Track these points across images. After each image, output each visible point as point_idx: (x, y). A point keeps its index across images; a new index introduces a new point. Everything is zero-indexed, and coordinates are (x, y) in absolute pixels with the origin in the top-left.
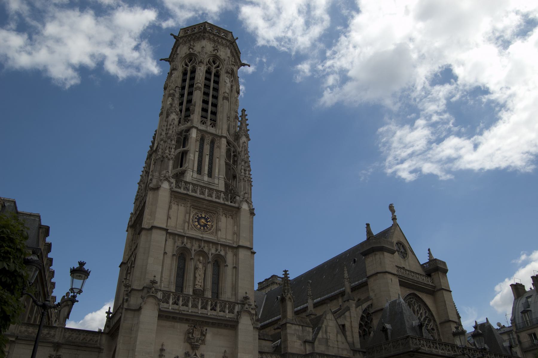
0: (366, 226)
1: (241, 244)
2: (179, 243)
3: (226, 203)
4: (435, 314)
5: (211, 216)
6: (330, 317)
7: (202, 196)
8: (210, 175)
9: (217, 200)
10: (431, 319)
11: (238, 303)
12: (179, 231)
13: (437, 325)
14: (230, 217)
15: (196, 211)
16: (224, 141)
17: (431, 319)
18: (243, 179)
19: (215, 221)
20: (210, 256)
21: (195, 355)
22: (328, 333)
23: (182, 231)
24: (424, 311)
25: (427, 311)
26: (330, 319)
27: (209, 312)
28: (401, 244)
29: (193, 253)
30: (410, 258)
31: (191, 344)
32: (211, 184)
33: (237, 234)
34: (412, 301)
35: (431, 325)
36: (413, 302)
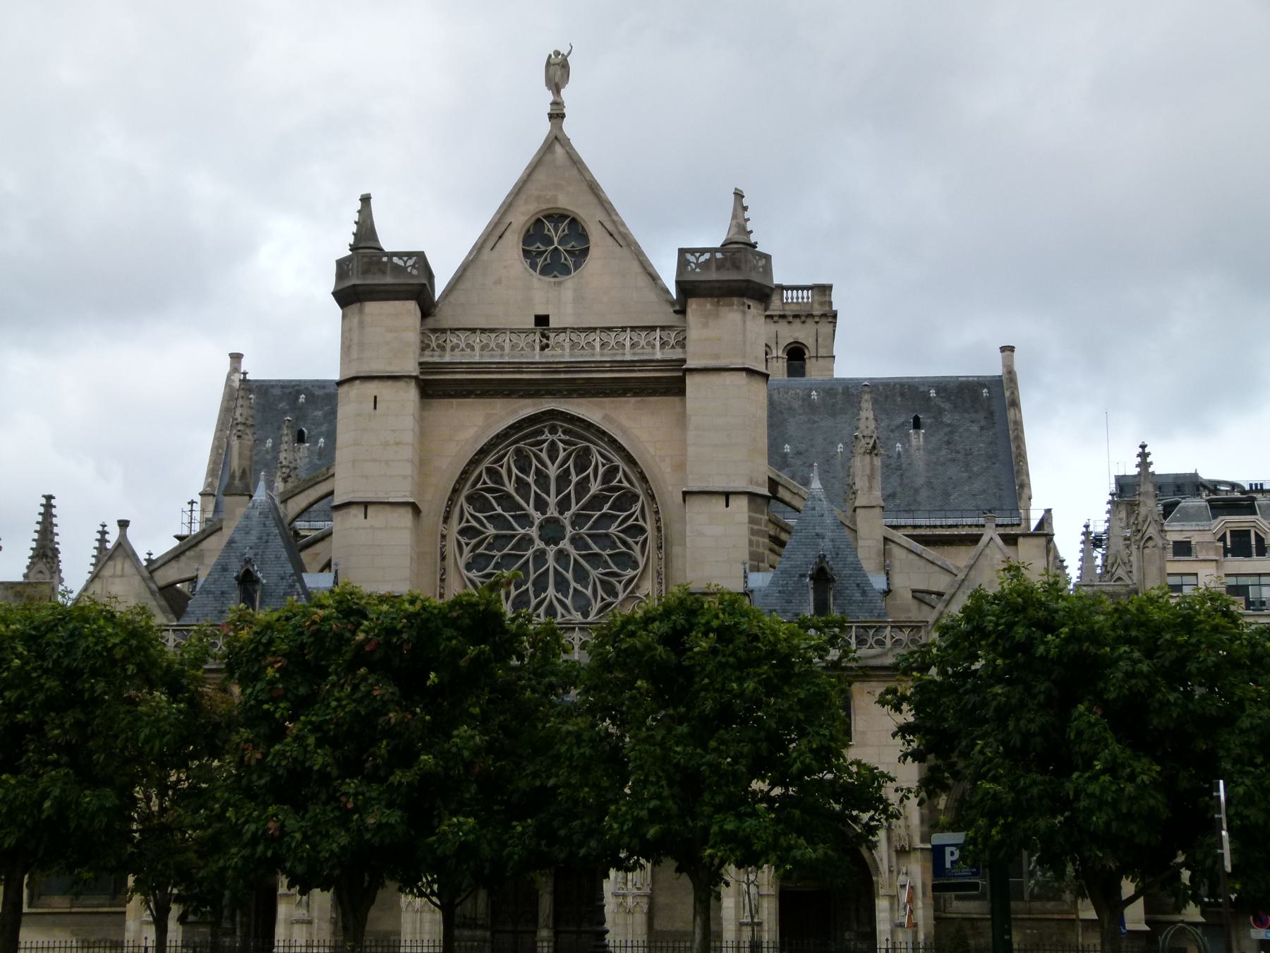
0: (358, 205)
4: (669, 470)
6: (119, 566)
10: (639, 491)
13: (657, 512)
24: (601, 470)
25: (617, 461)
26: (119, 572)
28: (567, 217)
30: (593, 263)
34: (544, 441)
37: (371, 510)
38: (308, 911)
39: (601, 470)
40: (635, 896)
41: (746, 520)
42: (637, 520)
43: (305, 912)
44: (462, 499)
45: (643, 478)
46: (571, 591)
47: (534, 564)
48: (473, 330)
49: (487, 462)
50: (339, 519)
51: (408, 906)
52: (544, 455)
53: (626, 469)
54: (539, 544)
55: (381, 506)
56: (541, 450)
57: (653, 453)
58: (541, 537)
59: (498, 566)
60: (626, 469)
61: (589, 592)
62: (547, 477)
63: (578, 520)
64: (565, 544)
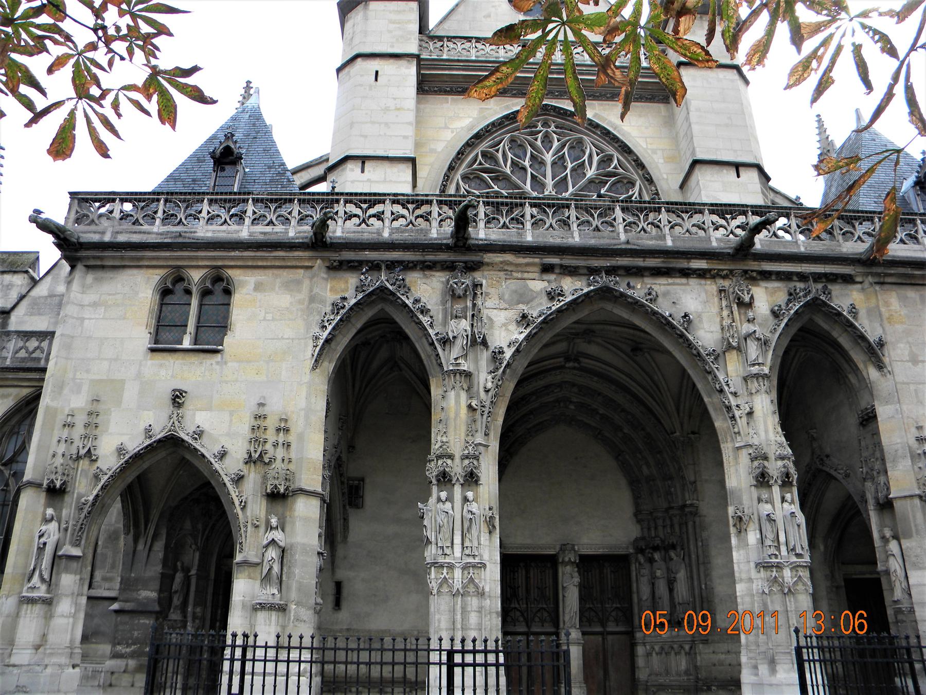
4: (661, 161)
10: (636, 177)
17: (636, 177)
37: (368, 165)
38: (280, 591)
39: (596, 159)
40: (795, 567)
43: (276, 592)
44: (458, 176)
45: (640, 165)
48: (468, 39)
49: (484, 146)
51: (441, 585)
53: (620, 157)
55: (379, 162)
57: (645, 147)
60: (620, 157)
62: (542, 163)
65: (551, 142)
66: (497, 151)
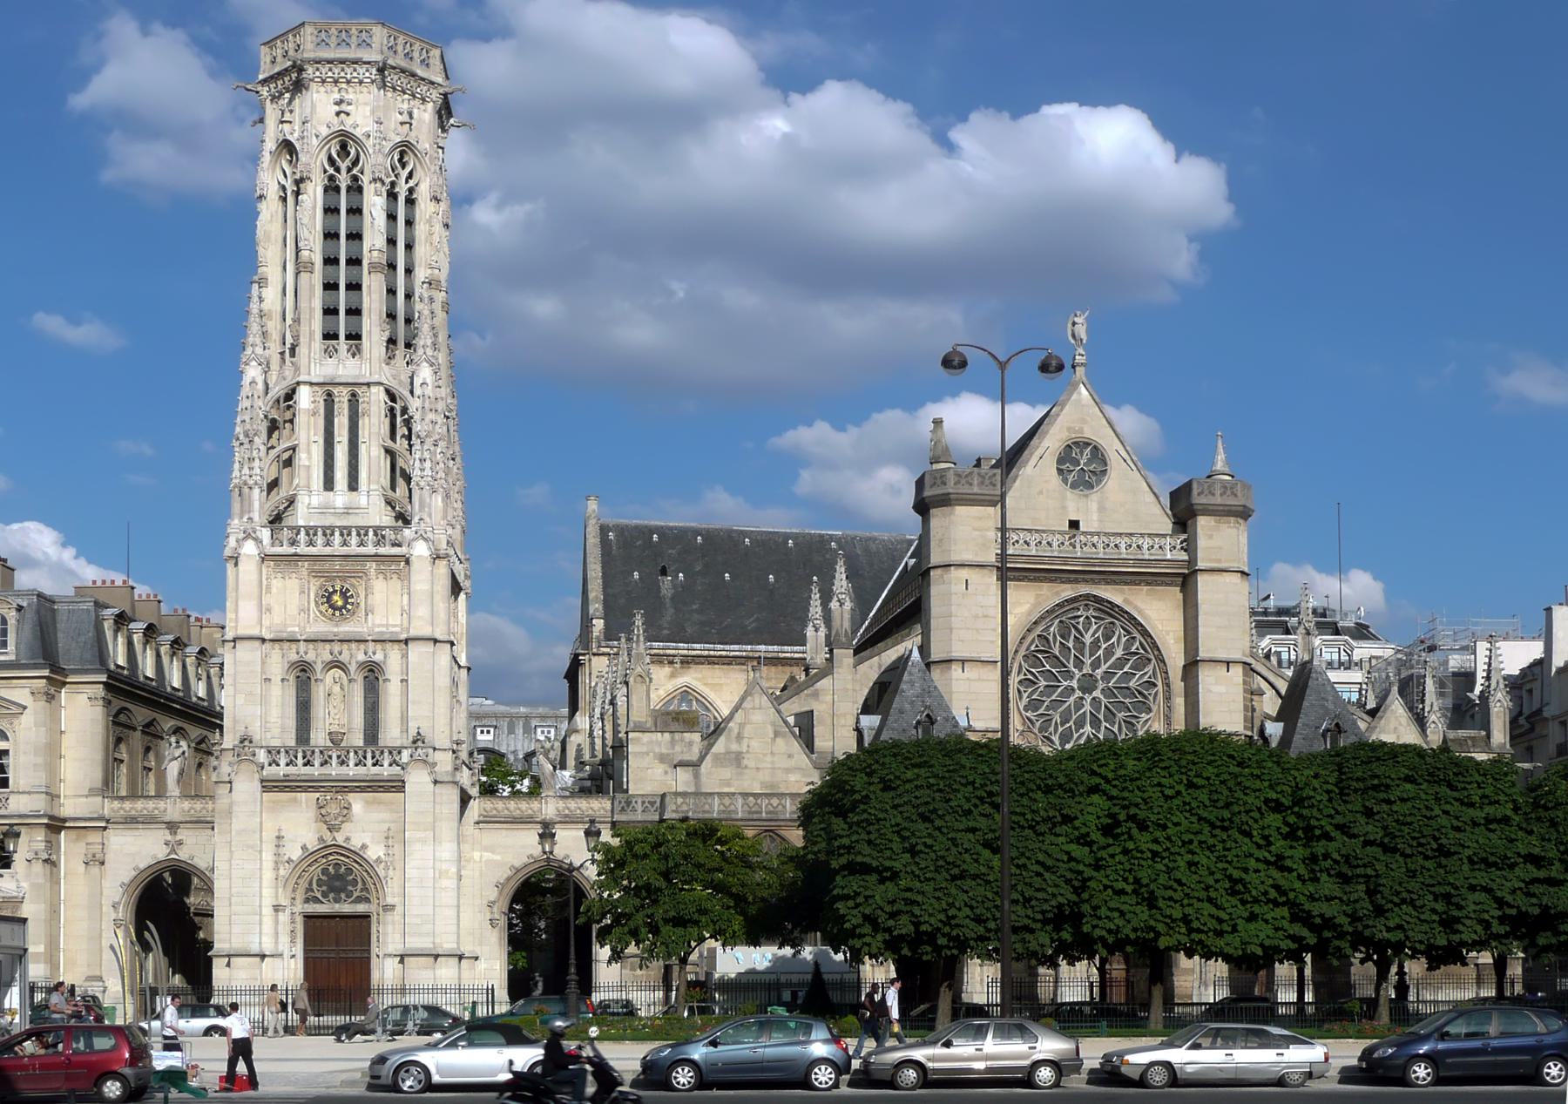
1: (413, 633)
2: (294, 657)
3: (382, 550)
4: (1172, 641)
5: (353, 586)
7: (328, 550)
8: (353, 485)
9: (362, 550)
11: (406, 748)
12: (293, 629)
13: (1166, 673)
14: (395, 576)
15: (322, 579)
16: (378, 395)
17: (1153, 657)
18: (418, 485)
19: (362, 596)
20: (353, 668)
21: (334, 839)
22: (746, 740)
23: (297, 629)
24: (1124, 639)
27: (351, 770)
29: (319, 667)
31: (325, 822)
32: (350, 511)
33: (407, 613)
34: (1079, 617)
35: (1146, 673)
36: (1081, 619)
41: (1241, 682)
42: (1150, 677)
45: (1155, 646)
46: (1103, 728)
47: (1070, 711)
50: (938, 671)
52: (1080, 627)
54: (1078, 694)
56: (1078, 623)
58: (1079, 688)
59: (1048, 708)
61: (1115, 730)
62: (1084, 643)
63: (1108, 675)
64: (1097, 693)
65: (1090, 623)
66: (1049, 634)
